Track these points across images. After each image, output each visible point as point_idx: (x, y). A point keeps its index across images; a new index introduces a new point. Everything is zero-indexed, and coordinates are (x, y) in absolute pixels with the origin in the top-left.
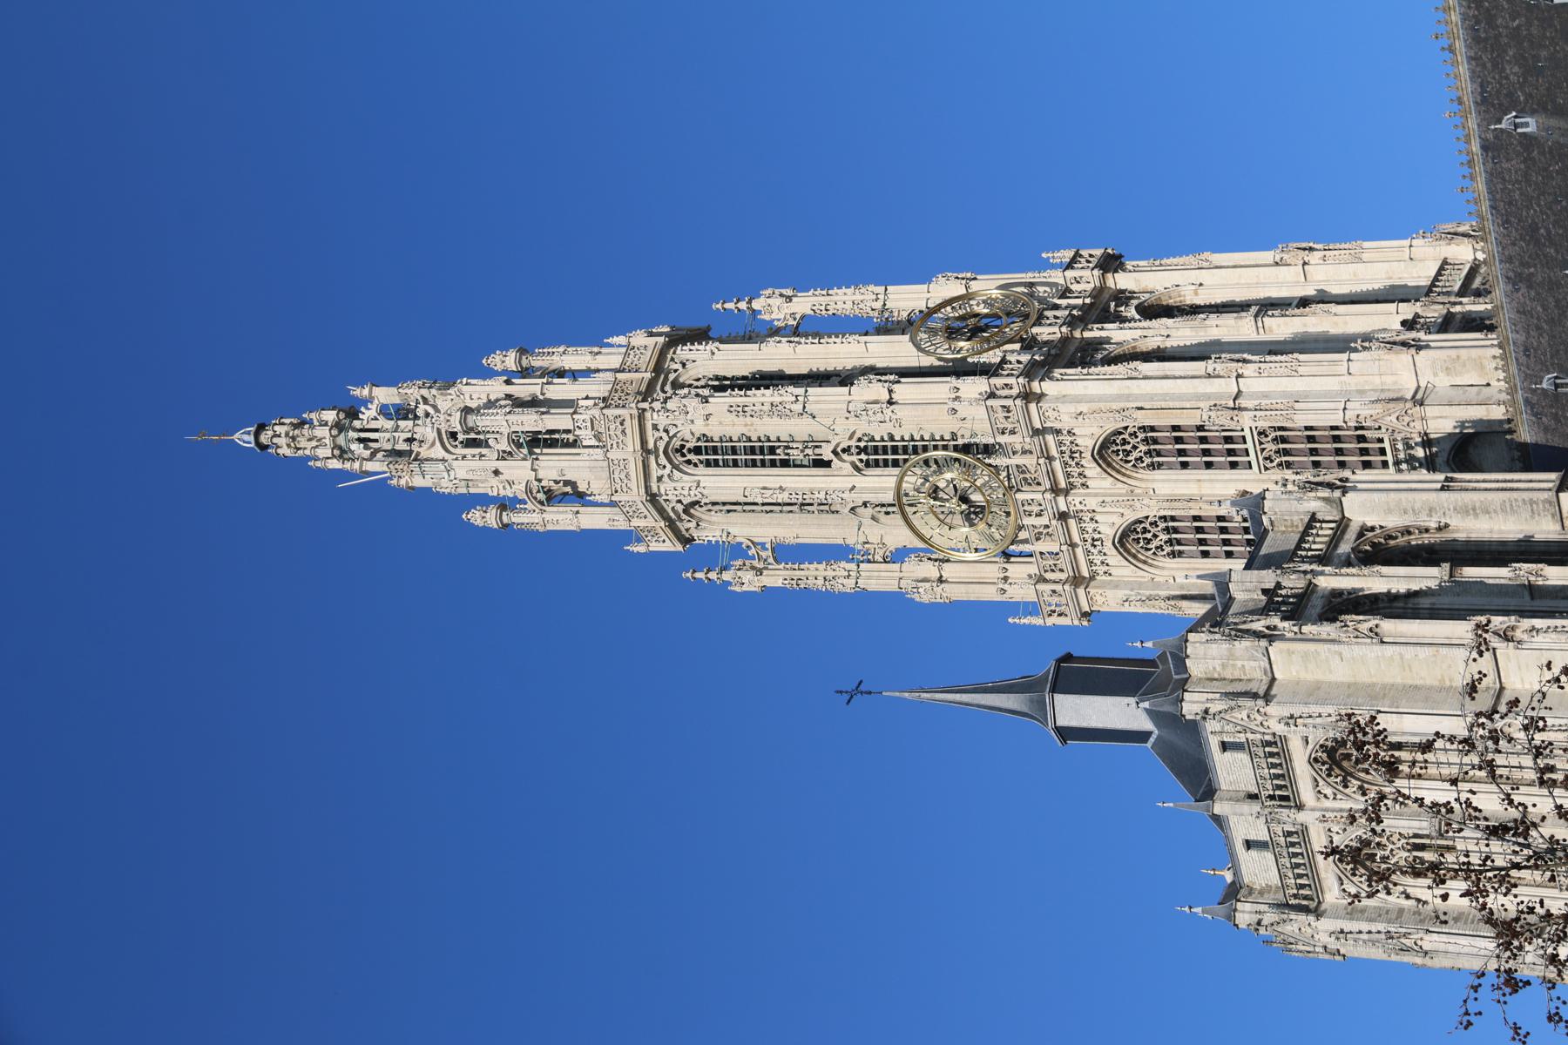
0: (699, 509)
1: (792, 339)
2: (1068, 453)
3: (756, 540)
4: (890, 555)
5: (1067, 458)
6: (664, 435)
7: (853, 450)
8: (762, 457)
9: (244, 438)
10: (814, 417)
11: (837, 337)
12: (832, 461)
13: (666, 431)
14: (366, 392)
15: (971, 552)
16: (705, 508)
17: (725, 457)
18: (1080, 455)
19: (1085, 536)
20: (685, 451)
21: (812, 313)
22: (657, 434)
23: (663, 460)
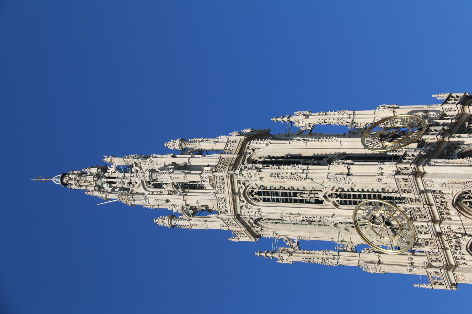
0: (262, 221)
1: (305, 138)
2: (440, 202)
3: (290, 237)
4: (355, 248)
5: (439, 205)
6: (243, 186)
7: (334, 196)
8: (290, 198)
9: (56, 180)
10: (312, 180)
11: (327, 138)
12: (323, 201)
13: (244, 184)
14: (109, 160)
15: (393, 250)
16: (264, 221)
17: (273, 197)
18: (446, 204)
19: (452, 244)
20: (253, 193)
21: (318, 124)
22: (240, 185)
23: (243, 198)
